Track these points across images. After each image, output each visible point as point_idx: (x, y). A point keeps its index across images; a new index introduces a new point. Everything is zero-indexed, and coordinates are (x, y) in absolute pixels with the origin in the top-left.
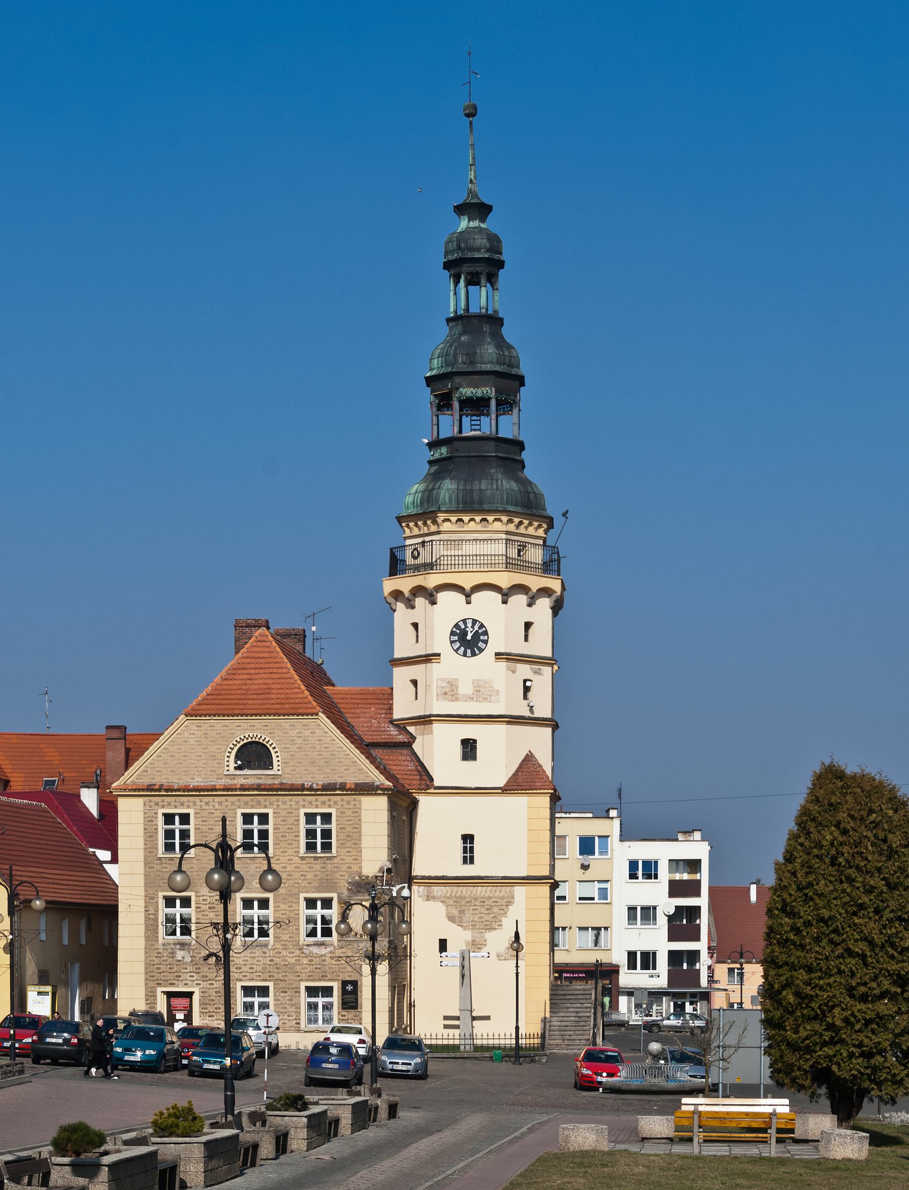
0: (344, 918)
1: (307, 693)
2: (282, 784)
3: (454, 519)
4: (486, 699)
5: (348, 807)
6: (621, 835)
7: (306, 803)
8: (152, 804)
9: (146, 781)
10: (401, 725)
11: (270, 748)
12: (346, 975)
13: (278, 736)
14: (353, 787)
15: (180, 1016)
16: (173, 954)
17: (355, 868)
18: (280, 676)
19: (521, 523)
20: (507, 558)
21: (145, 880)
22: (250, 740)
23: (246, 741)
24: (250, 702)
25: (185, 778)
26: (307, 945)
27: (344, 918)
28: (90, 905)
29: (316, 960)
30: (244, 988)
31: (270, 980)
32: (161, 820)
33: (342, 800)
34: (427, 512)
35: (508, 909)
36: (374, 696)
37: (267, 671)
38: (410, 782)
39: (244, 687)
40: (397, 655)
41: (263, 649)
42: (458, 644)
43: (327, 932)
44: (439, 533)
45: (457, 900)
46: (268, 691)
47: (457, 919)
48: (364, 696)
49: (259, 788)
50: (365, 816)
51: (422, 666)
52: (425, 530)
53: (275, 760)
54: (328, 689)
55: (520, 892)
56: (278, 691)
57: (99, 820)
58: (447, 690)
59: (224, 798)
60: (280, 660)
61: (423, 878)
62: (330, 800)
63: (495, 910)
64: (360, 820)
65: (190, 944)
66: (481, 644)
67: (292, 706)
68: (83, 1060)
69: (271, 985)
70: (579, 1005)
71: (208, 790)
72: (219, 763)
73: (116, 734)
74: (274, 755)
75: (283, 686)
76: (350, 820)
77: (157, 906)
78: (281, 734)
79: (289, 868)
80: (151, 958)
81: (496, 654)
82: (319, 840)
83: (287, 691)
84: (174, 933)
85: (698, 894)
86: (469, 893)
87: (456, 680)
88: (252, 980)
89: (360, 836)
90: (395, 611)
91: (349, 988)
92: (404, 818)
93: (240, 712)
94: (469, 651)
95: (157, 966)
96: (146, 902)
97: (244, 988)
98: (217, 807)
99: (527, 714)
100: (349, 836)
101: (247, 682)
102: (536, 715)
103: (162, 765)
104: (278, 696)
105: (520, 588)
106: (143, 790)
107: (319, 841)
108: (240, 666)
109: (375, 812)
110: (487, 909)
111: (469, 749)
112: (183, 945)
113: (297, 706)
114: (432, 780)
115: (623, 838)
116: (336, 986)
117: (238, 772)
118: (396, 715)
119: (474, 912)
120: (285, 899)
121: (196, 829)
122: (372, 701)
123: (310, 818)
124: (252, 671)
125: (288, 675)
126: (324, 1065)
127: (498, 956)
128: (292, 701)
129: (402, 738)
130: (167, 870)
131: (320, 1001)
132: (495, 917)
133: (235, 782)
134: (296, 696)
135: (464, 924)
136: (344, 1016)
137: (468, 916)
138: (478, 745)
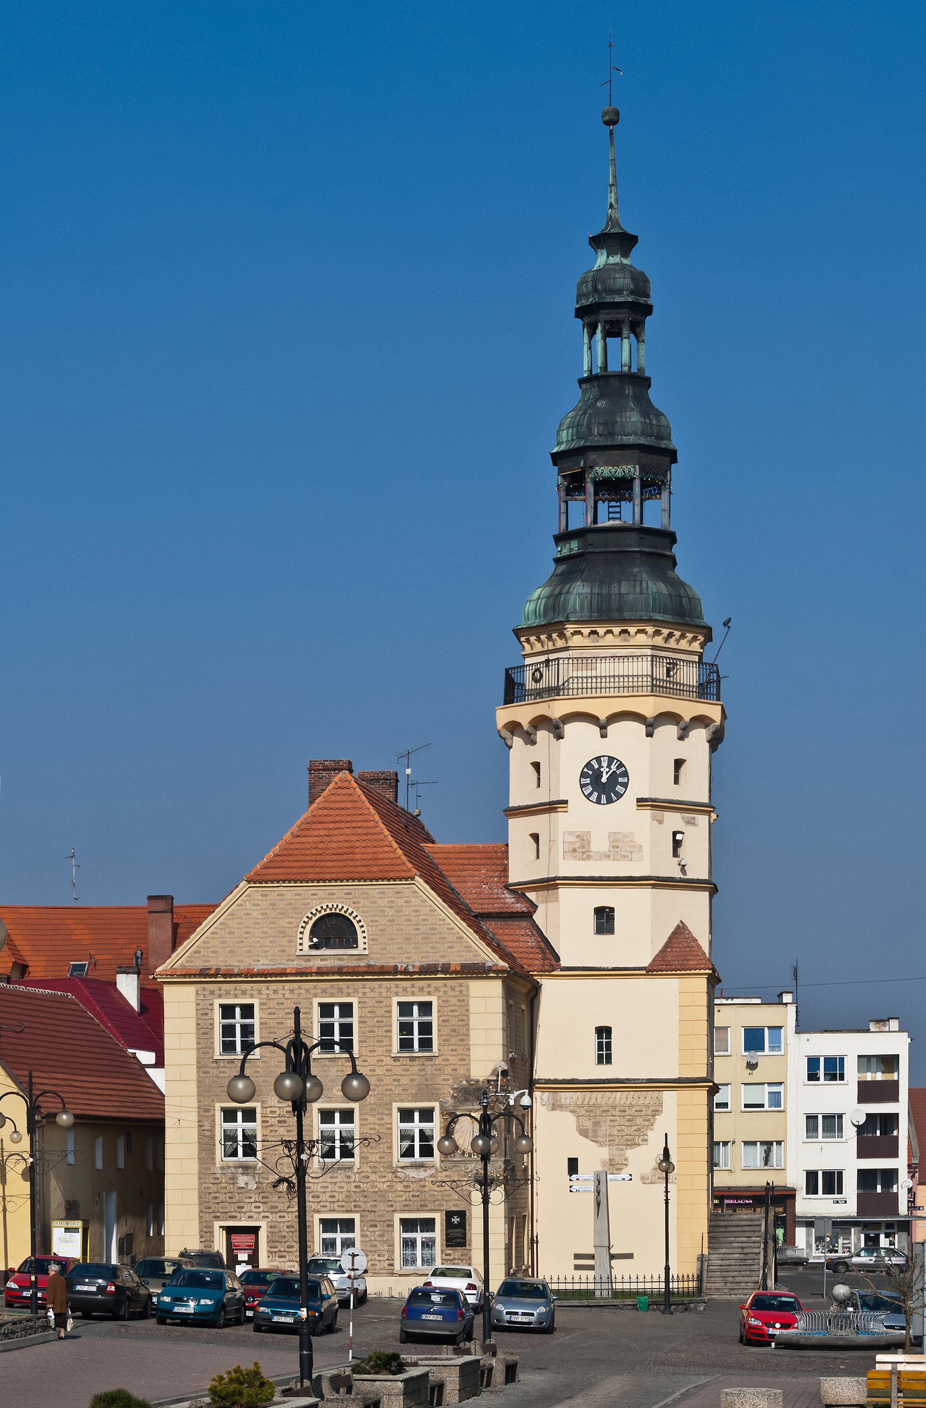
0: (448, 1133)
1: (400, 852)
2: (369, 966)
3: (586, 631)
4: (627, 857)
5: (453, 993)
6: (797, 1026)
7: (400, 990)
8: (206, 993)
9: (198, 964)
10: (519, 891)
11: (355, 922)
12: (451, 1204)
13: (364, 906)
14: (459, 968)
15: (243, 1256)
16: (234, 1179)
17: (462, 1071)
18: (365, 831)
19: (670, 635)
20: (653, 679)
22: (328, 911)
23: (323, 913)
24: (329, 864)
25: (247, 960)
26: (402, 1168)
27: (448, 1133)
28: (129, 1119)
29: (413, 1186)
30: (323, 1222)
31: (356, 1212)
32: (217, 1013)
33: (445, 986)
34: (552, 623)
36: (484, 855)
37: (349, 825)
38: (530, 962)
39: (321, 846)
40: (513, 803)
41: (344, 798)
42: (590, 789)
43: (427, 1151)
44: (567, 649)
45: (591, 1109)
46: (351, 850)
47: (590, 1134)
48: (472, 855)
49: (340, 971)
50: (474, 1005)
51: (545, 816)
52: (550, 646)
53: (360, 936)
54: (427, 846)
55: (670, 1098)
56: (364, 850)
57: (140, 1014)
58: (576, 846)
59: (296, 985)
60: (366, 812)
61: (548, 1081)
62: (429, 986)
63: (639, 1121)
64: (467, 1010)
65: (255, 1168)
66: (619, 788)
67: (381, 868)
68: (122, 1313)
69: (357, 1217)
70: (745, 1239)
71: (276, 975)
72: (290, 941)
73: (161, 906)
74: (359, 931)
75: (370, 844)
76: (456, 1011)
77: (214, 1121)
78: (368, 904)
79: (379, 1071)
80: (206, 1185)
81: (639, 800)
82: (416, 1035)
83: (375, 850)
84: (234, 1154)
85: (895, 1098)
86: (605, 1100)
88: (333, 1211)
89: (468, 1030)
90: (510, 747)
91: (456, 1220)
92: (523, 1007)
93: (316, 877)
94: (604, 797)
96: (199, 1115)
97: (323, 1222)
98: (287, 996)
99: (678, 875)
100: (454, 1031)
101: (325, 839)
102: (690, 876)
103: (219, 945)
104: (364, 857)
105: (669, 717)
106: (195, 975)
107: (416, 1037)
108: (315, 819)
109: (487, 1000)
110: (629, 1120)
111: (605, 919)
112: (246, 1169)
113: (388, 868)
114: (558, 959)
115: (799, 1030)
116: (439, 1218)
117: (314, 952)
118: (513, 878)
121: (261, 1023)
122: (483, 861)
123: (405, 1008)
124: (331, 826)
125: (375, 830)
126: (424, 1317)
128: (380, 862)
129: (520, 907)
130: (225, 1075)
131: (419, 1236)
132: (639, 1130)
133: (310, 964)
134: (387, 855)
135: (600, 1139)
136: (449, 1255)
137: (604, 1129)
138: (616, 914)
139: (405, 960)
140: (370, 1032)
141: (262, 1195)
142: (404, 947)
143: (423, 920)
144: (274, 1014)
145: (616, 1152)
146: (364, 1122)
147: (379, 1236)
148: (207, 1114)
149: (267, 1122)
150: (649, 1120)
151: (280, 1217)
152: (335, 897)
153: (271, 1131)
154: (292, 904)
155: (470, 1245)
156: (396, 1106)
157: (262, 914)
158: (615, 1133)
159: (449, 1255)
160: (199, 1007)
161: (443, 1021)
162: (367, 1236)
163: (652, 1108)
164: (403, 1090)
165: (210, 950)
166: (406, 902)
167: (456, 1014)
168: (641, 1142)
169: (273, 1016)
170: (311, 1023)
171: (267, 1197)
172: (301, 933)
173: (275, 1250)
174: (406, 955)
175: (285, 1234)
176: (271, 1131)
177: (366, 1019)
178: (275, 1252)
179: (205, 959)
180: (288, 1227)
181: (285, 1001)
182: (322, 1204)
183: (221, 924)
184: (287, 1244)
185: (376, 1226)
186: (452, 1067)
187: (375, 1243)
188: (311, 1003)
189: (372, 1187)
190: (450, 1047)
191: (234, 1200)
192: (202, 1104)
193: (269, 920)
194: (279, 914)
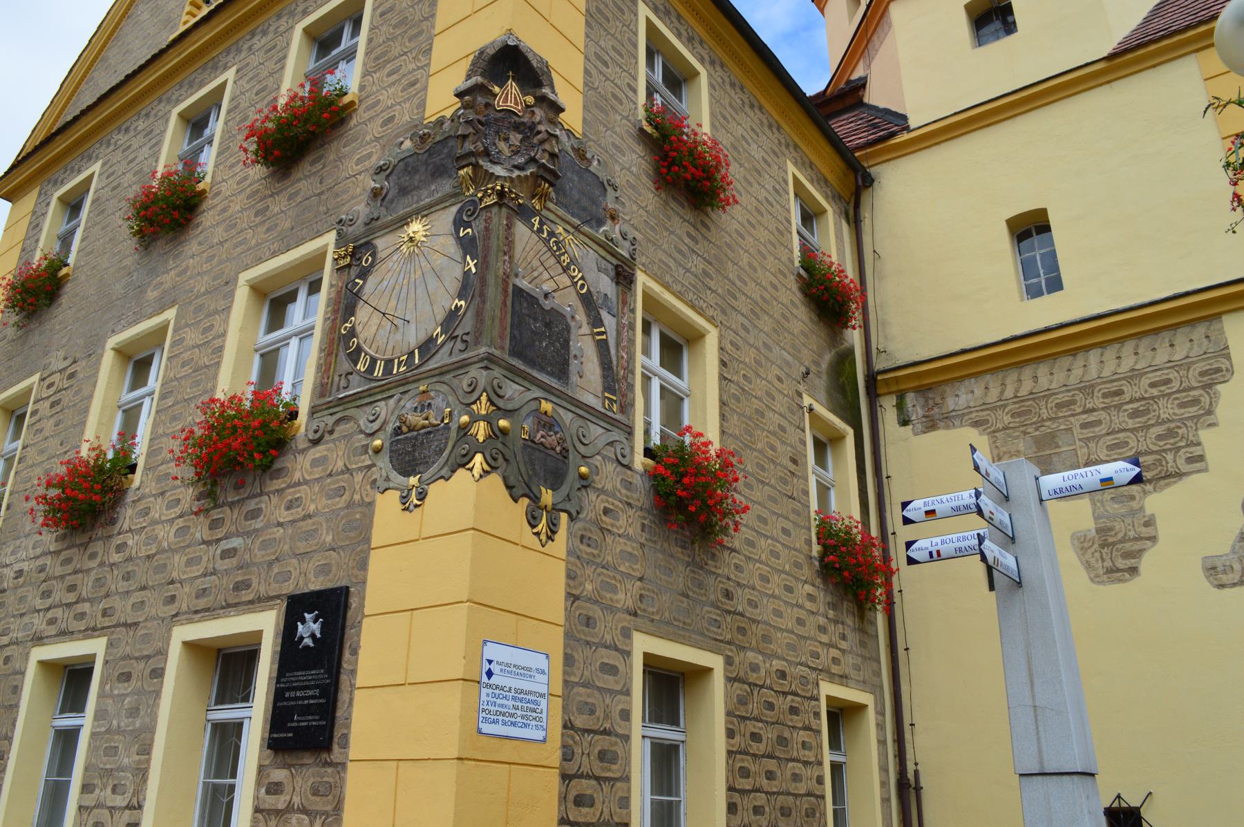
12: (311, 565)
17: (404, 116)
45: (1023, 409)
91: (309, 628)
110: (1135, 414)
119: (1088, 433)
127: (1211, 570)
132: (1171, 433)
150: (1195, 402)
155: (345, 745)
168: (1185, 468)
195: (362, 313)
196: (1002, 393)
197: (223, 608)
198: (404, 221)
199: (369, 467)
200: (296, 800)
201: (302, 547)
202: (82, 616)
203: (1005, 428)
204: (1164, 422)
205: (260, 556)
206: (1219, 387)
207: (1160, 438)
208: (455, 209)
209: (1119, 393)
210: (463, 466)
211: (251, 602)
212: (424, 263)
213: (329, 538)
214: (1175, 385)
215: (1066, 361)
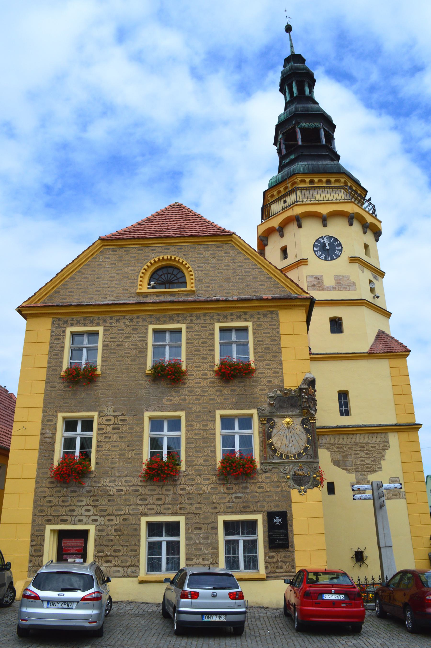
12: (272, 504)
17: (276, 382)
21: (45, 399)
27: (266, 435)
31: (181, 514)
35: (385, 453)
58: (315, 283)
63: (374, 454)
64: (278, 332)
69: (182, 519)
72: (132, 283)
87: (322, 276)
91: (278, 520)
95: (48, 498)
97: (150, 525)
100: (268, 349)
110: (367, 454)
111: (336, 325)
119: (356, 456)
120: (199, 416)
121: (104, 346)
132: (375, 460)
136: (272, 557)
139: (225, 295)
140: (195, 351)
141: (93, 498)
142: (224, 285)
143: (239, 266)
144: (115, 338)
145: (361, 477)
146: (190, 428)
147: (204, 538)
148: (50, 423)
149: (102, 429)
150: (381, 453)
151: (109, 520)
152: (169, 251)
153: (106, 437)
154: (135, 257)
156: (218, 413)
157: (111, 264)
158: (359, 463)
159: (272, 557)
160: (53, 334)
161: (258, 341)
162: (191, 539)
163: (382, 445)
164: (225, 399)
165: (67, 290)
166: (225, 253)
167: (268, 335)
168: (377, 470)
169: (114, 340)
170: (146, 345)
171: (97, 501)
172: (141, 277)
173: (102, 554)
174: (225, 291)
175: (112, 537)
176: (106, 437)
177: (193, 341)
178: (102, 557)
179: (63, 297)
180: (116, 530)
181: (125, 328)
182: (149, 507)
183: (78, 271)
184: (114, 548)
185: (200, 529)
186: (268, 379)
187: (199, 546)
188: (147, 329)
189: (197, 489)
190: (265, 363)
191: (66, 504)
192: (46, 414)
193: (117, 268)
194: (125, 264)
195: (274, 439)
196: (334, 441)
197: (239, 512)
198: (285, 417)
199: (286, 482)
200: (279, 559)
201: (268, 499)
202: (169, 509)
203: (335, 451)
204: (373, 457)
205: (251, 500)
206: (386, 451)
207: (372, 461)
208: (301, 419)
209: (363, 447)
210: (316, 487)
211: (251, 512)
212: (293, 431)
213: (277, 498)
214: (377, 448)
215: (351, 436)
